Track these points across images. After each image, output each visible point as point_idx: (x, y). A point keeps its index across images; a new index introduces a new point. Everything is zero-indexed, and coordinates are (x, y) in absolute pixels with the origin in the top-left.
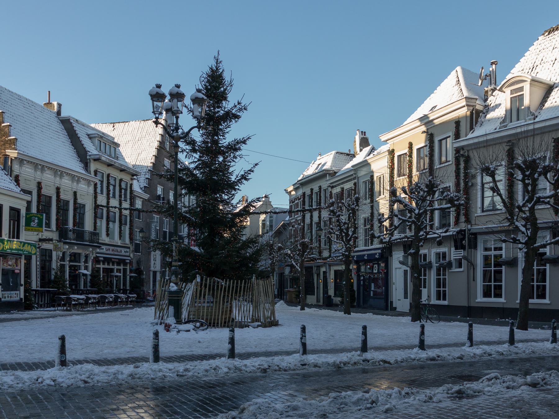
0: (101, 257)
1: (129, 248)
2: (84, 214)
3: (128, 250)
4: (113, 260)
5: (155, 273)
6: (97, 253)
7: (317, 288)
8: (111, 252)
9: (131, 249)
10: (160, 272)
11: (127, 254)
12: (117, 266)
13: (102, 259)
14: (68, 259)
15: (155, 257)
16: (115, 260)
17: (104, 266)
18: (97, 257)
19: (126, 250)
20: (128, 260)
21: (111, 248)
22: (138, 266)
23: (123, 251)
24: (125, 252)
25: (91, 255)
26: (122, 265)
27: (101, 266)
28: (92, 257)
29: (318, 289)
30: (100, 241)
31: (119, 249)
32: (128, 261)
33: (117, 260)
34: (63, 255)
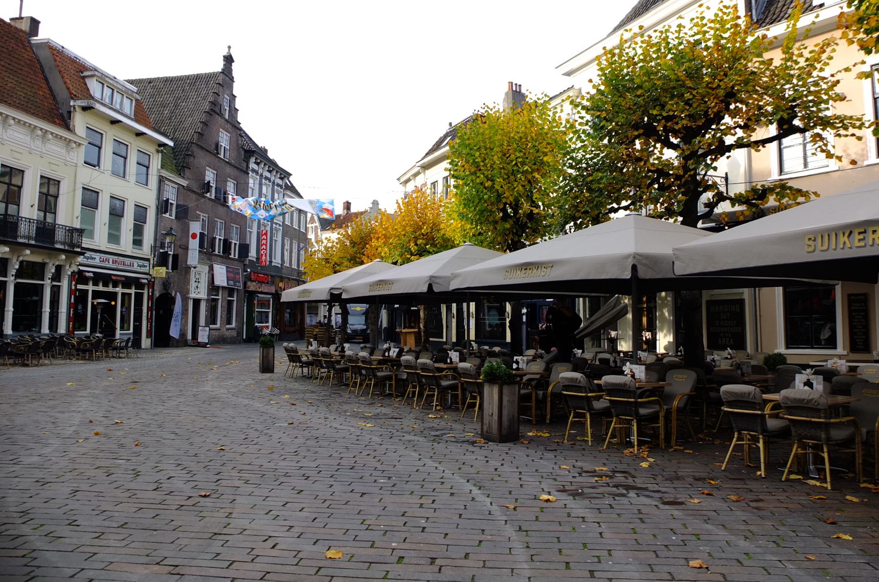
0: (89, 272)
1: (148, 260)
2: (56, 197)
3: (146, 263)
4: (114, 278)
5: (197, 302)
6: (81, 265)
7: (447, 326)
8: (111, 265)
9: (152, 262)
10: (207, 300)
11: (146, 270)
12: (93, 285)
13: (91, 275)
14: (14, 272)
15: (197, 276)
16: (119, 278)
17: (96, 288)
18: (81, 272)
19: (141, 262)
20: (144, 279)
21: (111, 258)
22: (165, 289)
23: (136, 265)
24: (139, 266)
25: (67, 267)
26: (134, 288)
27: (90, 288)
28: (68, 270)
29: (449, 329)
30: (83, 245)
31: (128, 261)
32: (146, 281)
33: (123, 279)
34: (56, 270)
